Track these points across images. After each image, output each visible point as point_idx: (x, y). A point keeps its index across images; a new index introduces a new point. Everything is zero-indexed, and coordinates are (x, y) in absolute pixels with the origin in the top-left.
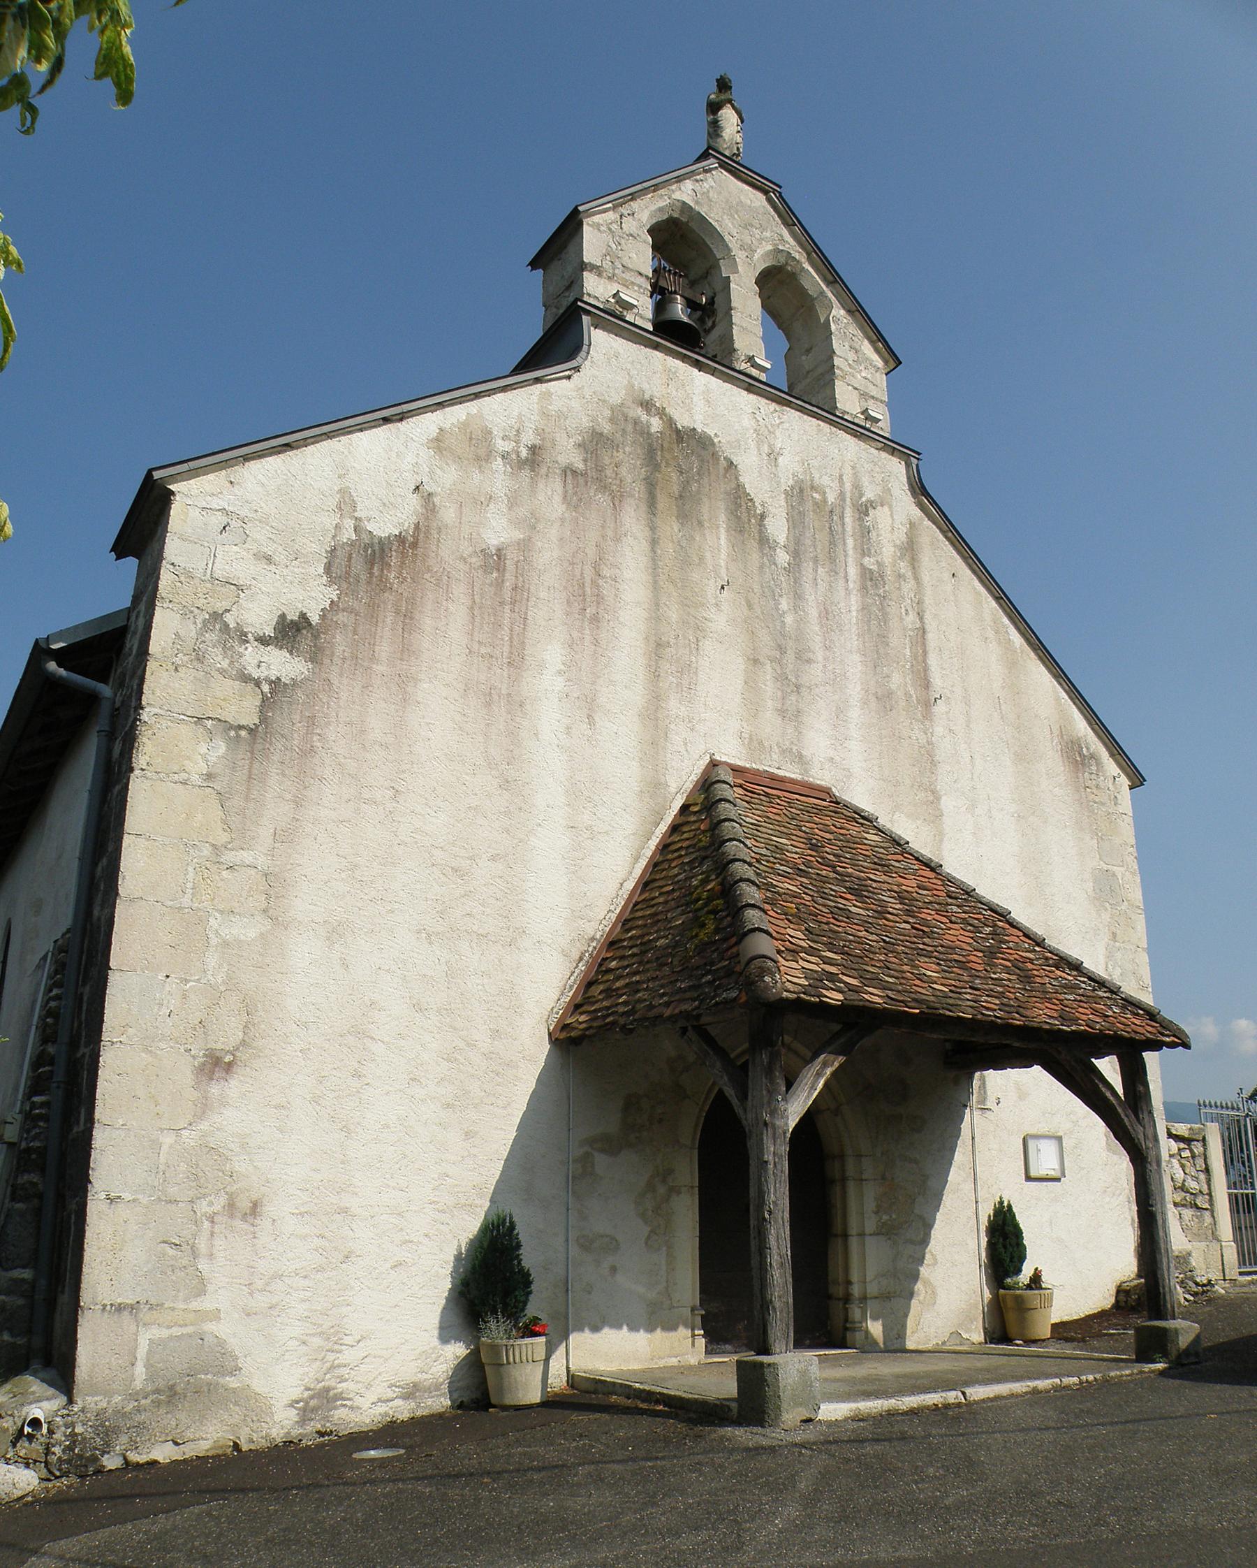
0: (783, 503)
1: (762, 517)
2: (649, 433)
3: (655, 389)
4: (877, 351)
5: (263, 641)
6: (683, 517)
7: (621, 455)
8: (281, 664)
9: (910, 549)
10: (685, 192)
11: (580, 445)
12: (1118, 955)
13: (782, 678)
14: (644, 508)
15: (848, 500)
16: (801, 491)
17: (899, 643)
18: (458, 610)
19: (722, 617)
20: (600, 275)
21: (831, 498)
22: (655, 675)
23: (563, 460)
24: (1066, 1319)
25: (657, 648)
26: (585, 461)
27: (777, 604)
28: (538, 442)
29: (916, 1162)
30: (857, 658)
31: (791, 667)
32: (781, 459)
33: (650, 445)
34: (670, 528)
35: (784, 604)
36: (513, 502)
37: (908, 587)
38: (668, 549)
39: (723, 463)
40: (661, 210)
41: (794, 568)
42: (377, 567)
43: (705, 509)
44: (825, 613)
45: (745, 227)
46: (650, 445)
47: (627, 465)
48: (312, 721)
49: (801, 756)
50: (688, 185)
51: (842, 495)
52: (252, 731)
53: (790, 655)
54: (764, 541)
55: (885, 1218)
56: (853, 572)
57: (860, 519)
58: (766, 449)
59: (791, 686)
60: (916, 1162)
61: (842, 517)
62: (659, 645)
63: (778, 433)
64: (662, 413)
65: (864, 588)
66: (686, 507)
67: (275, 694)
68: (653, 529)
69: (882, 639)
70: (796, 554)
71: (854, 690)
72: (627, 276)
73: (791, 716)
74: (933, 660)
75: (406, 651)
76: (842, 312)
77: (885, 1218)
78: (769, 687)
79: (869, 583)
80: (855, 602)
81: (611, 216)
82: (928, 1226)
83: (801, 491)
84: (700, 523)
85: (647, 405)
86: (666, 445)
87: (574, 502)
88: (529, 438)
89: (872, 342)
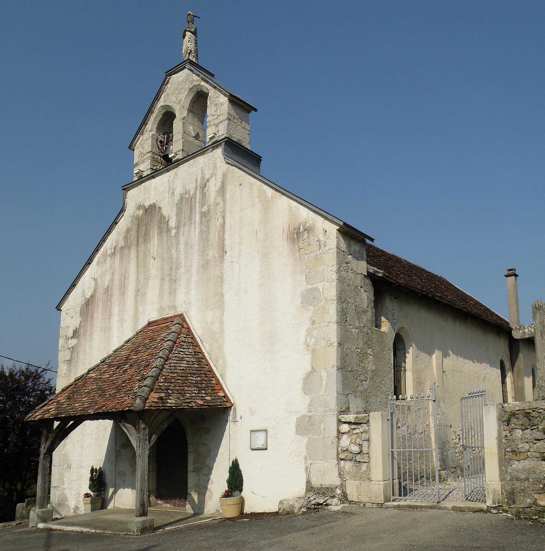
0: (175, 209)
1: (168, 221)
5: (71, 338)
8: (73, 342)
9: (222, 190)
12: (315, 332)
13: (171, 280)
14: (136, 246)
15: (199, 187)
16: (182, 199)
17: (214, 237)
18: (100, 309)
19: (154, 269)
22: (136, 302)
23: (120, 246)
24: (266, 511)
25: (138, 291)
27: (171, 252)
29: (207, 445)
30: (196, 254)
31: (174, 274)
35: (173, 251)
36: (111, 268)
37: (219, 209)
38: (141, 256)
40: (156, 117)
41: (177, 233)
42: (88, 306)
44: (187, 243)
48: (78, 353)
49: (175, 306)
51: (196, 188)
52: (69, 360)
53: (174, 270)
54: (169, 230)
55: (196, 466)
59: (173, 281)
60: (207, 445)
61: (195, 198)
62: (138, 291)
63: (176, 181)
67: (73, 349)
69: (207, 239)
70: (178, 228)
71: (194, 269)
72: (145, 157)
73: (173, 292)
74: (227, 234)
75: (92, 326)
77: (196, 466)
78: (166, 286)
80: (197, 231)
81: (141, 138)
82: (210, 469)
83: (182, 199)
84: (150, 240)
87: (121, 259)
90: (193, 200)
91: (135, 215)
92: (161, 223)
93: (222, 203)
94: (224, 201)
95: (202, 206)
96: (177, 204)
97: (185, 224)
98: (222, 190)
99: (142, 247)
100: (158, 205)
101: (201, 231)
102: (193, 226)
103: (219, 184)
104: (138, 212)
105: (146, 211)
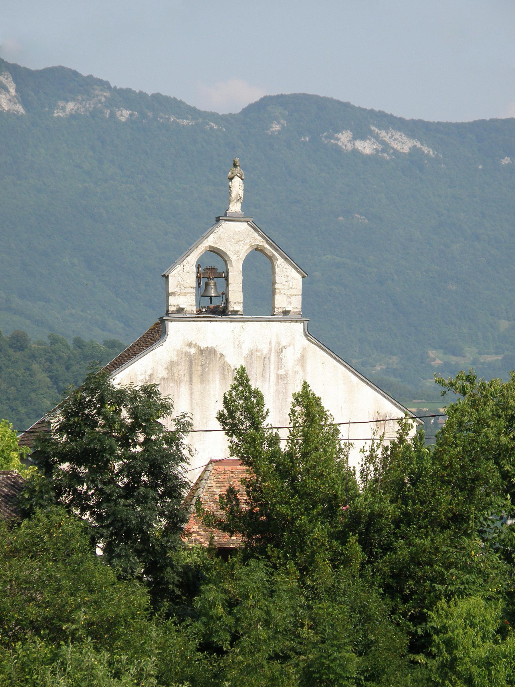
2: (190, 355)
3: (192, 338)
4: (298, 272)
6: (202, 381)
7: (180, 367)
9: (302, 360)
10: (210, 241)
11: (167, 368)
14: (188, 383)
15: (273, 350)
16: (252, 354)
20: (175, 296)
21: (265, 352)
23: (160, 376)
26: (168, 373)
28: (152, 372)
32: (243, 345)
33: (191, 360)
34: (197, 386)
38: (196, 395)
39: (219, 356)
43: (211, 376)
45: (237, 243)
46: (191, 360)
47: (182, 370)
50: (212, 236)
51: (270, 349)
56: (273, 378)
57: (278, 356)
58: (237, 343)
61: (269, 358)
64: (196, 346)
65: (278, 383)
66: (204, 378)
68: (191, 389)
72: (187, 290)
76: (283, 260)
79: (280, 380)
83: (252, 354)
84: (209, 381)
85: (190, 345)
86: (196, 357)
88: (149, 372)
89: (296, 269)
90: (266, 359)
91: (184, 350)
92: (224, 370)
93: (301, 373)
94: (304, 370)
95: (278, 369)
96: (245, 358)
97: (256, 379)
98: (302, 360)
99: (197, 386)
100: (219, 350)
101: (277, 392)
102: (267, 383)
103: (299, 356)
104: (188, 349)
105: (202, 352)
